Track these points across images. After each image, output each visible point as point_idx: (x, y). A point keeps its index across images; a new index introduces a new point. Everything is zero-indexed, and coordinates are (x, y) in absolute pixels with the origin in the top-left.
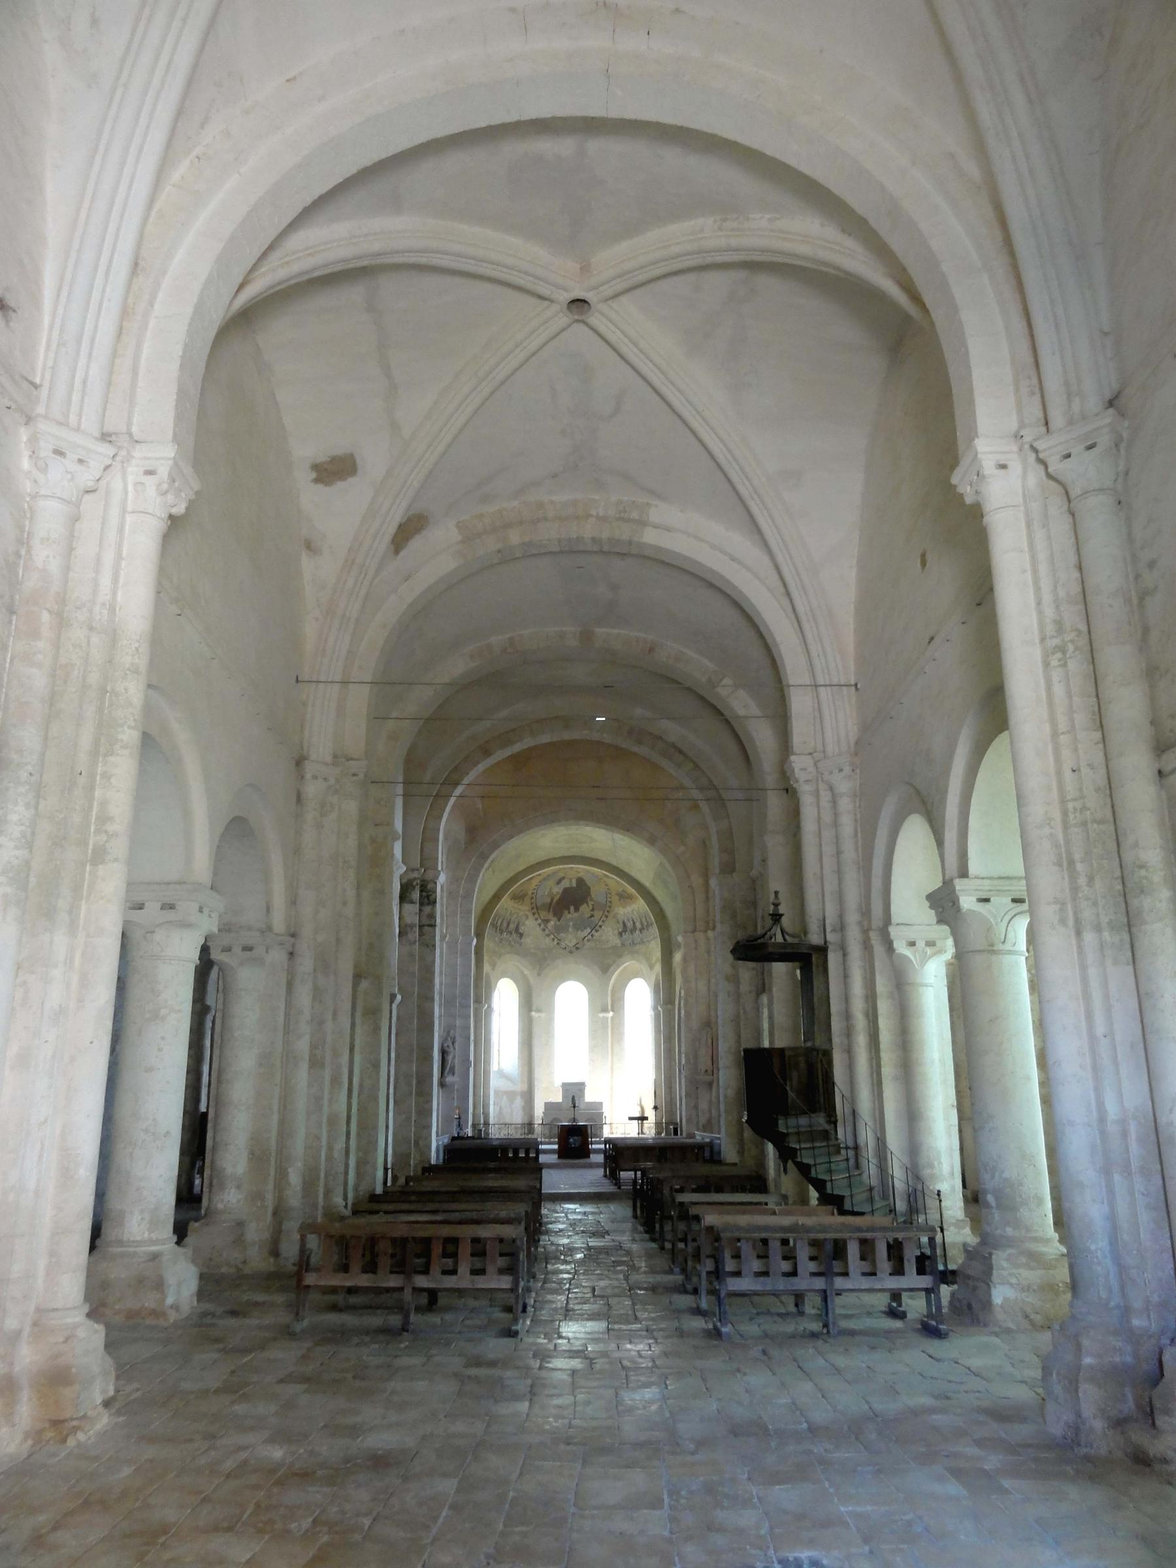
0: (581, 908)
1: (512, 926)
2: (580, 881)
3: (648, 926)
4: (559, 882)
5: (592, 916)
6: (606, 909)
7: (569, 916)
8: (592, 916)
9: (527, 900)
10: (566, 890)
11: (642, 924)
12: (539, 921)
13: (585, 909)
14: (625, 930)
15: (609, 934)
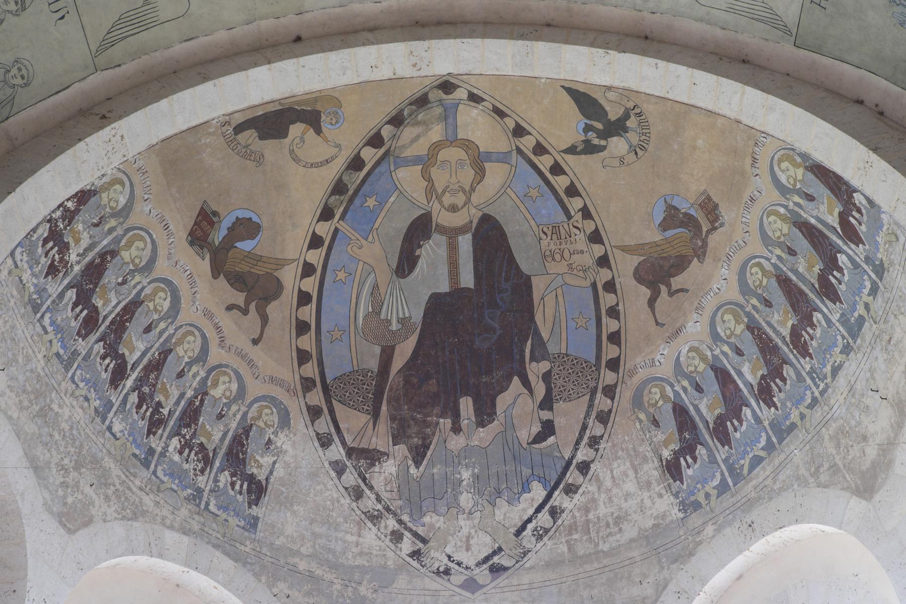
0: (503, 401)
1: (215, 434)
2: (490, 237)
3: (805, 318)
4: (406, 263)
5: (548, 429)
6: (602, 367)
7: (456, 443)
8: (548, 429)
9: (281, 311)
10: (436, 303)
11: (767, 348)
12: (337, 451)
13: (516, 403)
14: (688, 449)
15: (626, 485)
